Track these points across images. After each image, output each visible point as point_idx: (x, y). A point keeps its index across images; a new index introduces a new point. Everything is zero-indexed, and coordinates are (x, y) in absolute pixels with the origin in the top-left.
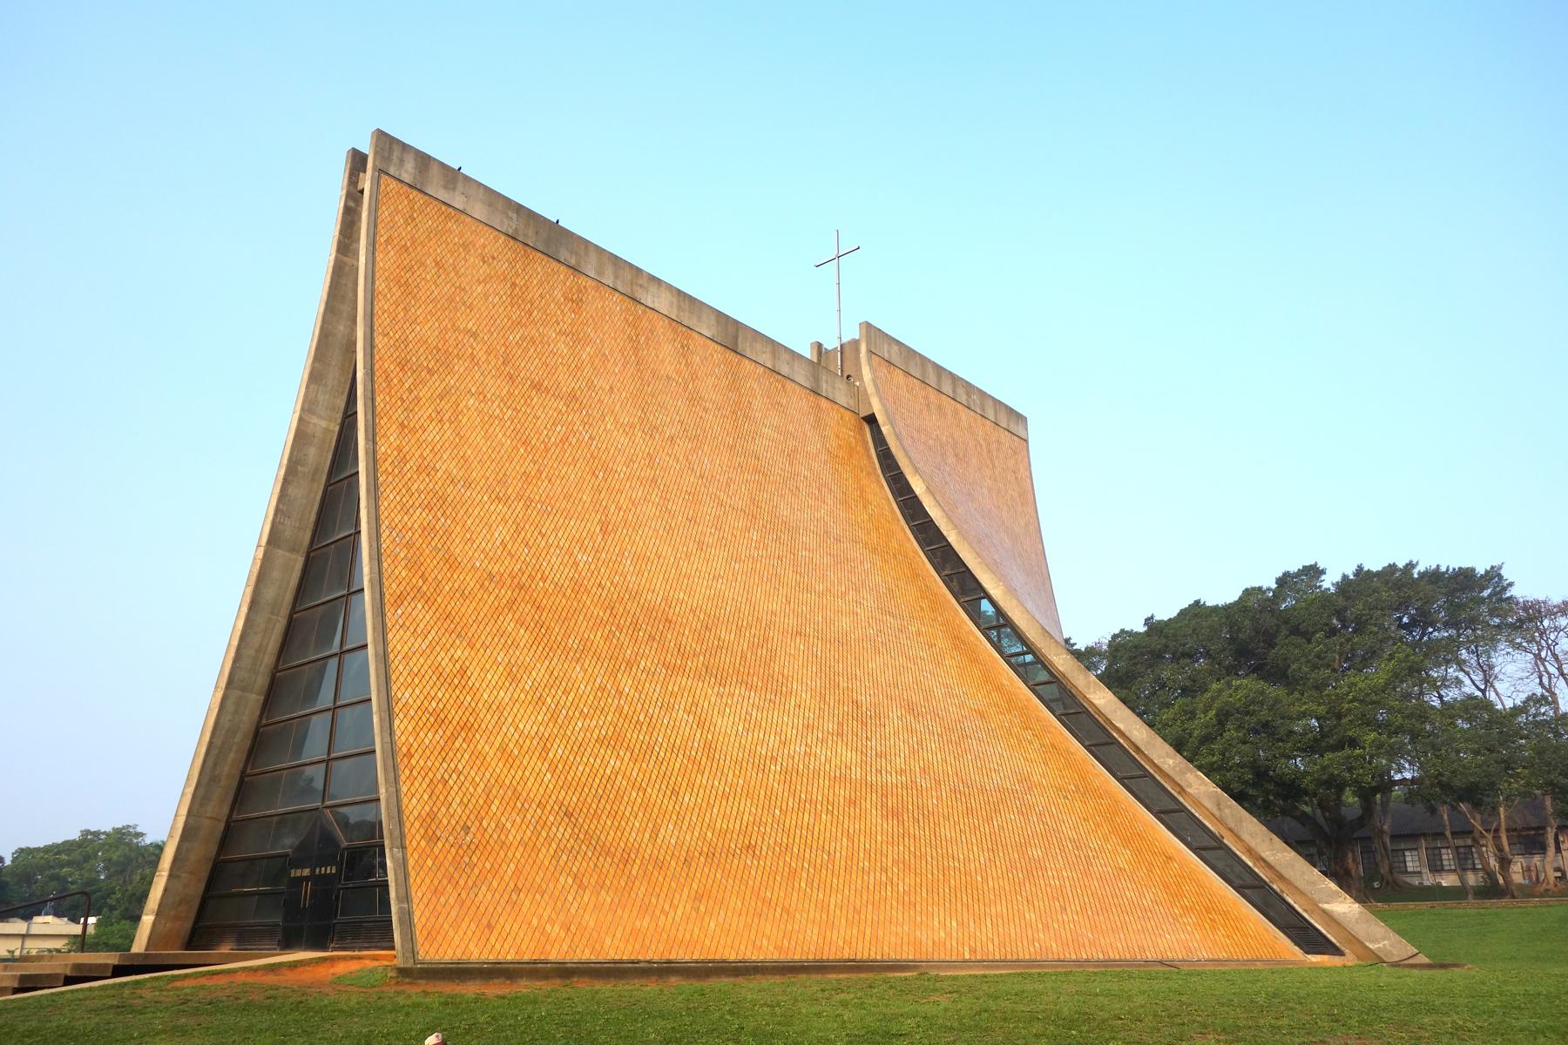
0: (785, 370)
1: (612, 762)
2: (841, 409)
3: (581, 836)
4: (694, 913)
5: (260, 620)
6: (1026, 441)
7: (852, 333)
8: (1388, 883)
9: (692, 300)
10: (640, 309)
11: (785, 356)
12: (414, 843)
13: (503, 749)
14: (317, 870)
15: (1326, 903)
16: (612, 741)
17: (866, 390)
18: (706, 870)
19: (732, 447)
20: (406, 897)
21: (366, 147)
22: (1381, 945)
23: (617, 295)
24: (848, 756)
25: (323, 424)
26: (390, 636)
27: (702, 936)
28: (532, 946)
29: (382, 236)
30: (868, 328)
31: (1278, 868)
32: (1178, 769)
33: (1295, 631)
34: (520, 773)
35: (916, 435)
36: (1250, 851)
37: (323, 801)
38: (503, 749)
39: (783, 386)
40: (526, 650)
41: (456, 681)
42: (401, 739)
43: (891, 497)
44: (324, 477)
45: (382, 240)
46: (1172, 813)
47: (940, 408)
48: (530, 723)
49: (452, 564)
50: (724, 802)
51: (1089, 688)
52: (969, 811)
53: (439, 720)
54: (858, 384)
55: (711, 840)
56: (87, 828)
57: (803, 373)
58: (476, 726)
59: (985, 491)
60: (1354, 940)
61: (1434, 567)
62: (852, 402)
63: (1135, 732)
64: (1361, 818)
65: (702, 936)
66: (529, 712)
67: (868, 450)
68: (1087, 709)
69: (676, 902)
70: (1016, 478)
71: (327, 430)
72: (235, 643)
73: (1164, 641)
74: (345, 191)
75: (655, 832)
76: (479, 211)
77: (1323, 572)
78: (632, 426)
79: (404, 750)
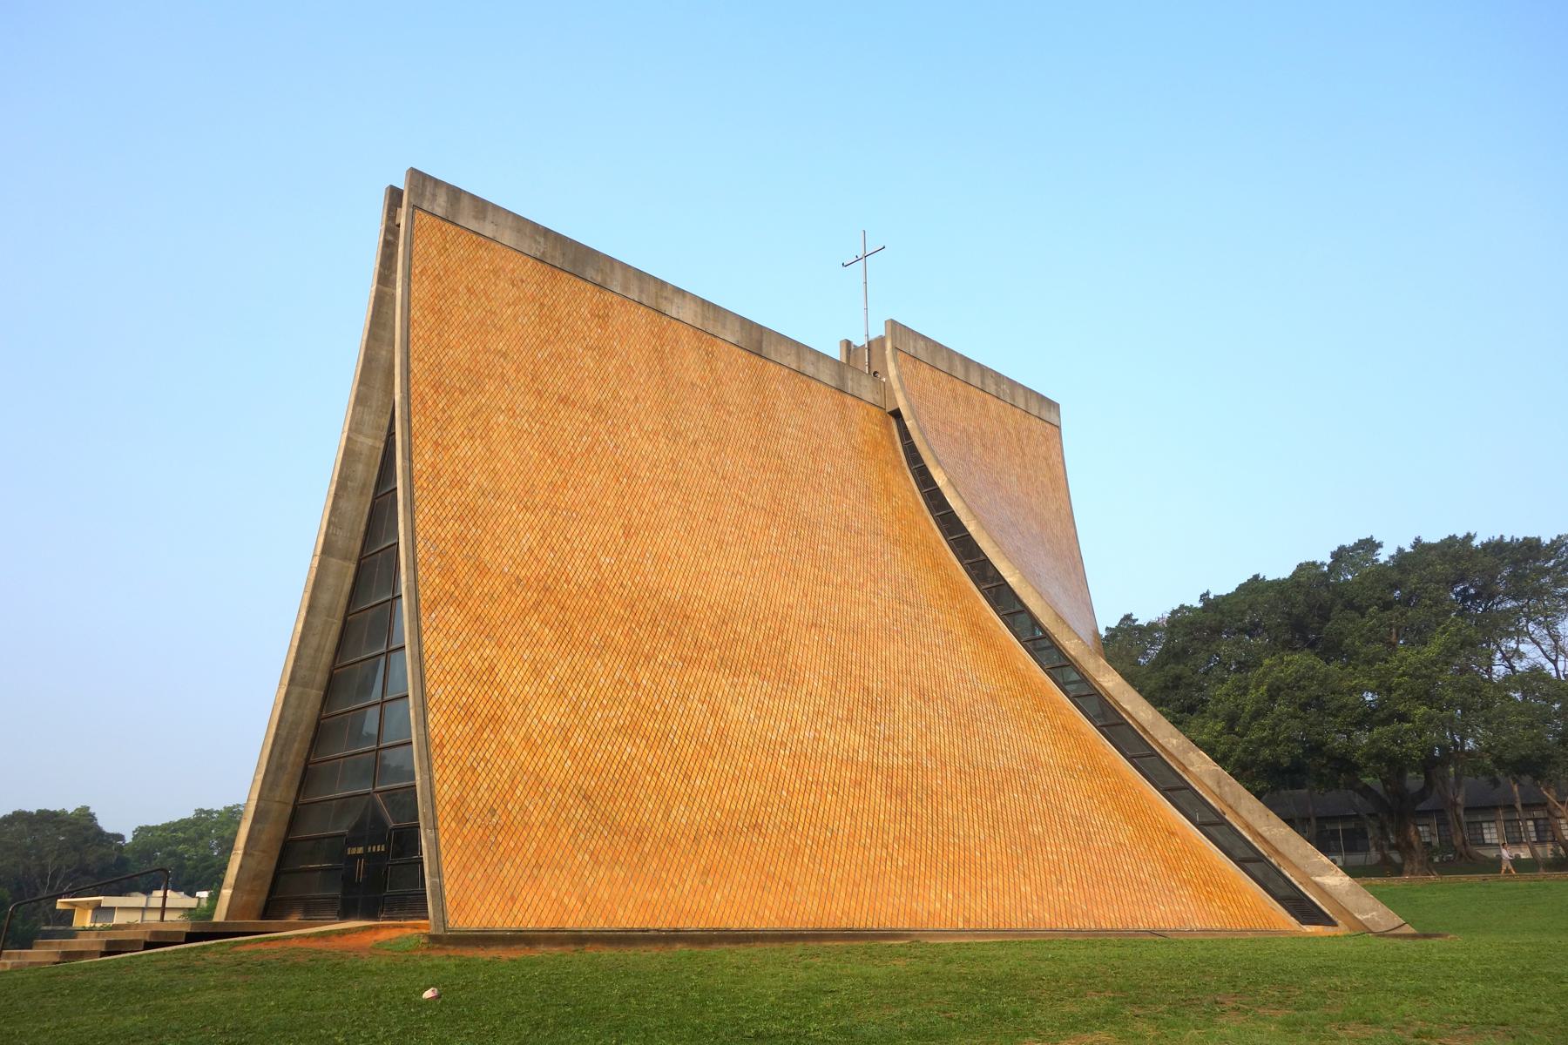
0: (810, 370)
1: (629, 750)
2: (868, 406)
3: (598, 817)
4: (701, 886)
5: (318, 622)
6: (1059, 427)
7: (878, 331)
8: (1461, 855)
9: (716, 308)
10: (665, 320)
11: (810, 357)
12: (445, 825)
13: (527, 738)
14: (369, 848)
16: (631, 730)
17: (891, 386)
18: (714, 847)
19: (755, 448)
20: (438, 873)
21: (401, 184)
22: (1369, 916)
23: (642, 308)
24: (856, 739)
25: (369, 442)
26: (425, 638)
27: (708, 908)
28: (551, 916)
29: (417, 267)
30: (893, 325)
32: (1181, 748)
33: (1350, 605)
34: (543, 760)
35: (941, 428)
36: (1248, 826)
37: (374, 787)
39: (808, 386)
40: (550, 648)
41: (485, 678)
42: (434, 731)
43: (916, 488)
44: (372, 491)
45: (417, 272)
46: (1176, 789)
47: (968, 400)
48: (553, 714)
49: (482, 570)
50: (733, 785)
51: (1099, 672)
52: (973, 790)
53: (469, 713)
54: (884, 380)
55: (720, 819)
56: (201, 807)
57: (829, 372)
58: (503, 718)
59: (1014, 479)
60: (1344, 911)
61: (1497, 537)
62: (878, 398)
63: (1142, 714)
64: (1423, 791)
65: (708, 908)
66: (551, 705)
67: (893, 443)
68: (1098, 692)
69: (684, 876)
70: (1048, 464)
71: (373, 448)
72: (296, 644)
73: (1219, 617)
74: (384, 226)
75: (667, 813)
76: (508, 238)
77: (1380, 545)
78: (656, 433)
79: (437, 741)
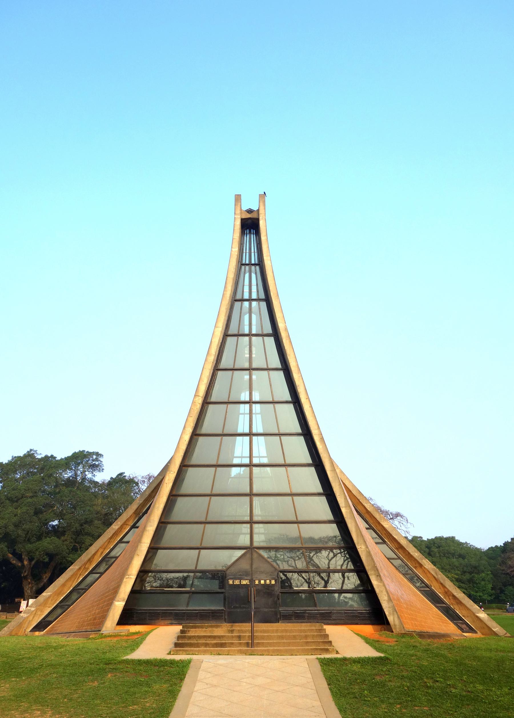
15: (478, 613)
22: (496, 630)
31: (460, 600)
32: (419, 557)
51: (381, 520)
63: (402, 541)
68: (373, 528)
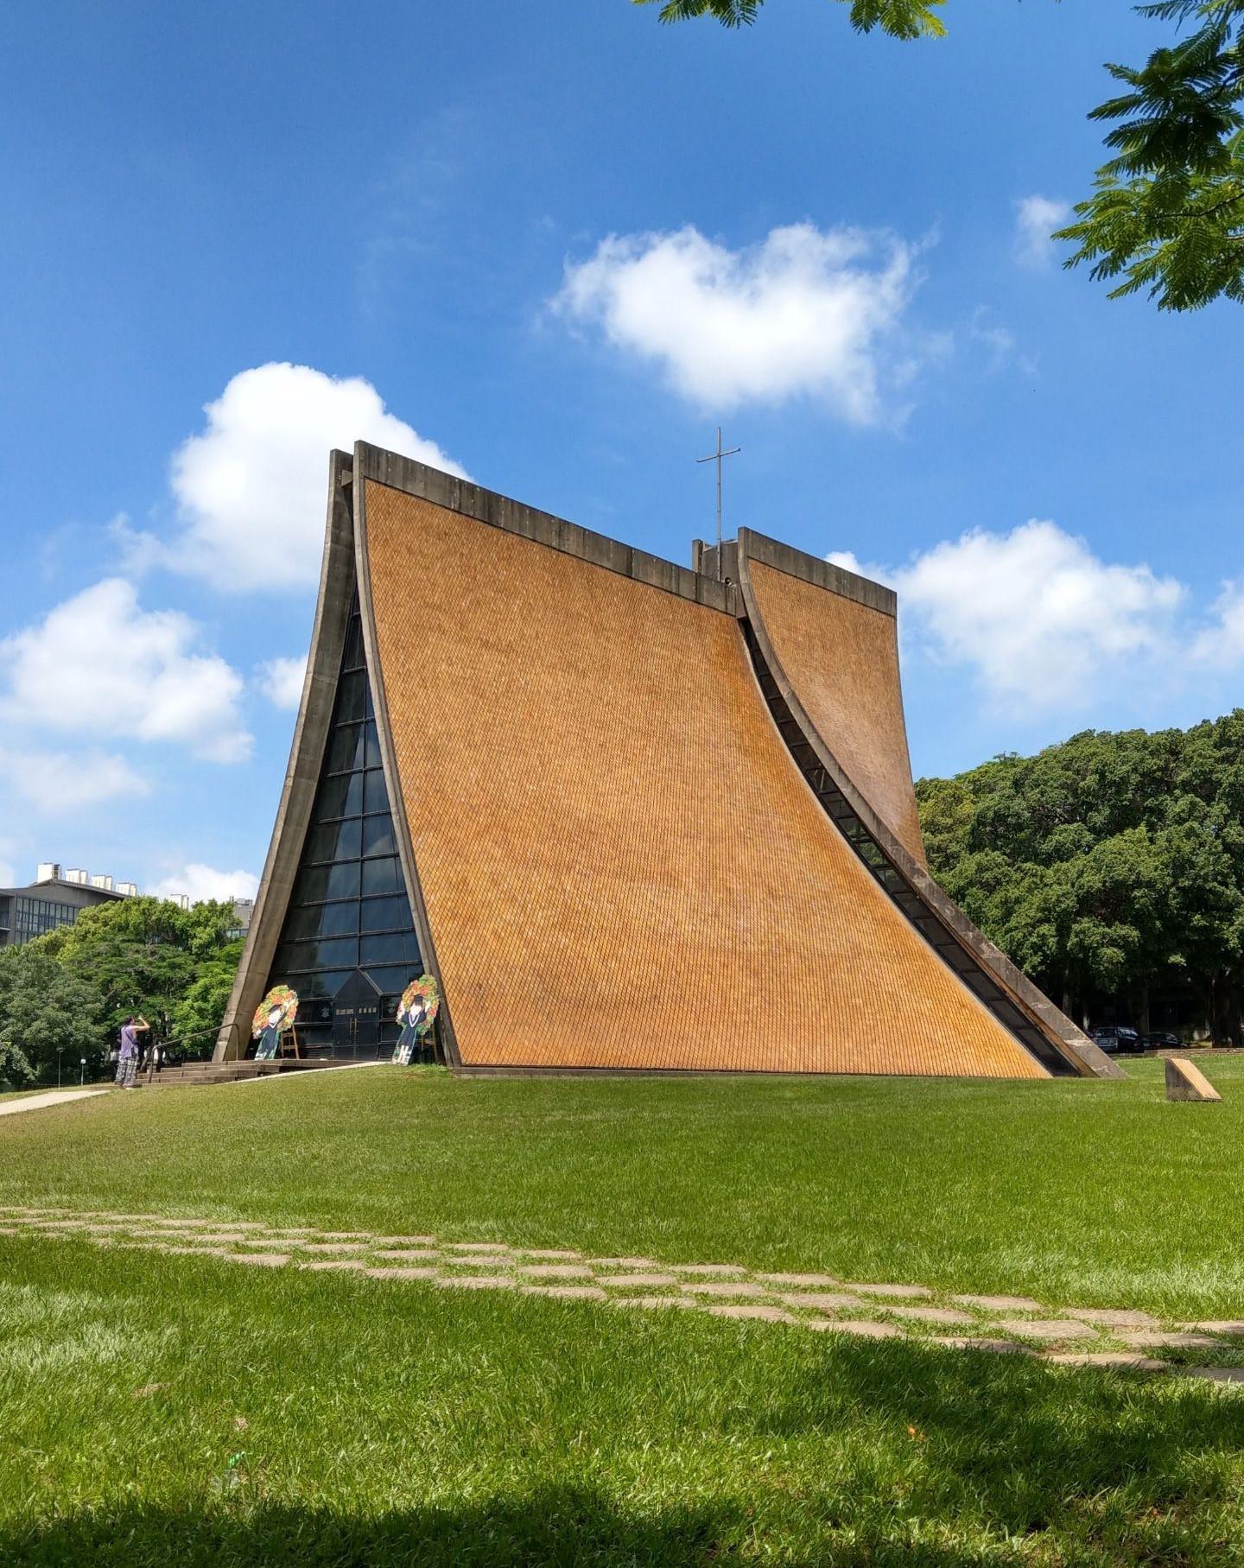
2: (720, 614)
5: (291, 830)
7: (731, 535)
14: (360, 1011)
16: (562, 925)
19: (629, 672)
21: (350, 449)
23: (536, 545)
26: (417, 858)
37: (359, 964)
38: (495, 933)
53: (454, 916)
79: (436, 935)
